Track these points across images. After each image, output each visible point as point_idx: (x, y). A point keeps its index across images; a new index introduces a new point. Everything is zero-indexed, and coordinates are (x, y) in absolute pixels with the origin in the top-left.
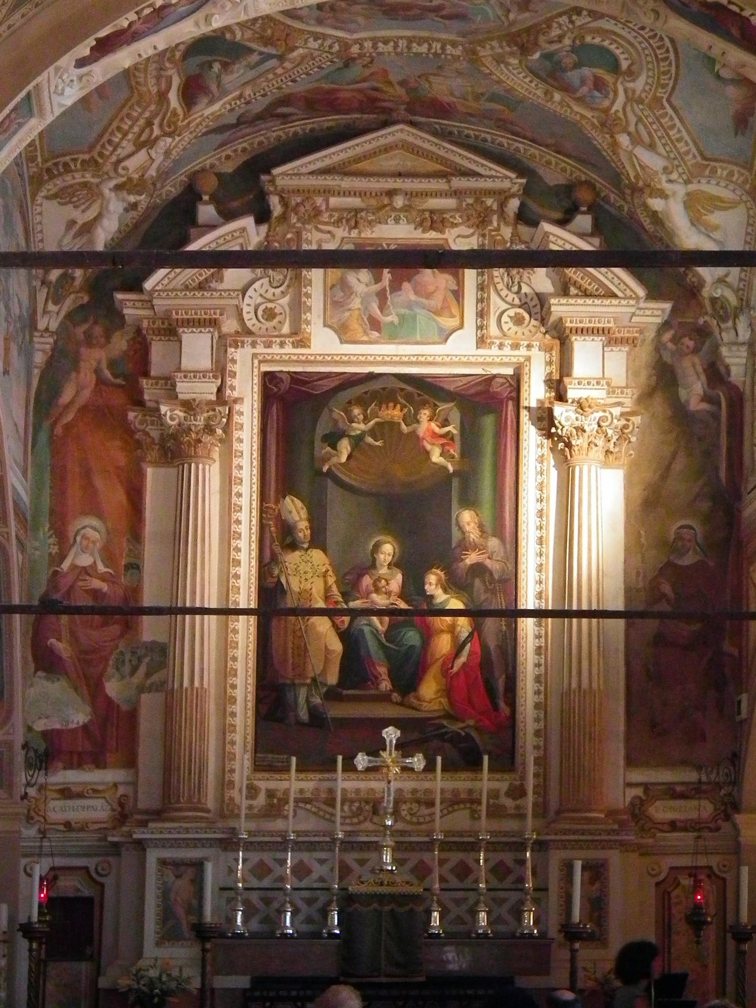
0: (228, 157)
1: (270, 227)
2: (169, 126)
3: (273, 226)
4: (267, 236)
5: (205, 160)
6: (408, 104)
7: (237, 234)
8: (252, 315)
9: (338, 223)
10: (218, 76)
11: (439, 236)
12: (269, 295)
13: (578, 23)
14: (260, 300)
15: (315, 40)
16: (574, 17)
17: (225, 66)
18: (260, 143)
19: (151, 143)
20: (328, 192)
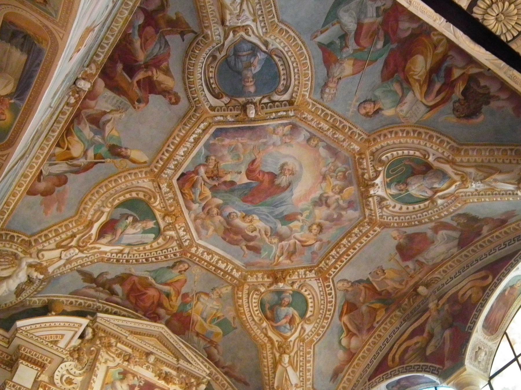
0: (71, 303)
1: (82, 342)
2: (83, 243)
3: (84, 342)
4: (80, 344)
5: (61, 297)
6: (175, 315)
7: (76, 325)
8: (59, 378)
9: (119, 355)
10: (126, 226)
11: (166, 385)
12: (72, 372)
13: (308, 276)
14: (65, 372)
15: (184, 231)
16: (308, 272)
17: (135, 221)
18: (89, 306)
19: (67, 248)
20: (119, 339)
